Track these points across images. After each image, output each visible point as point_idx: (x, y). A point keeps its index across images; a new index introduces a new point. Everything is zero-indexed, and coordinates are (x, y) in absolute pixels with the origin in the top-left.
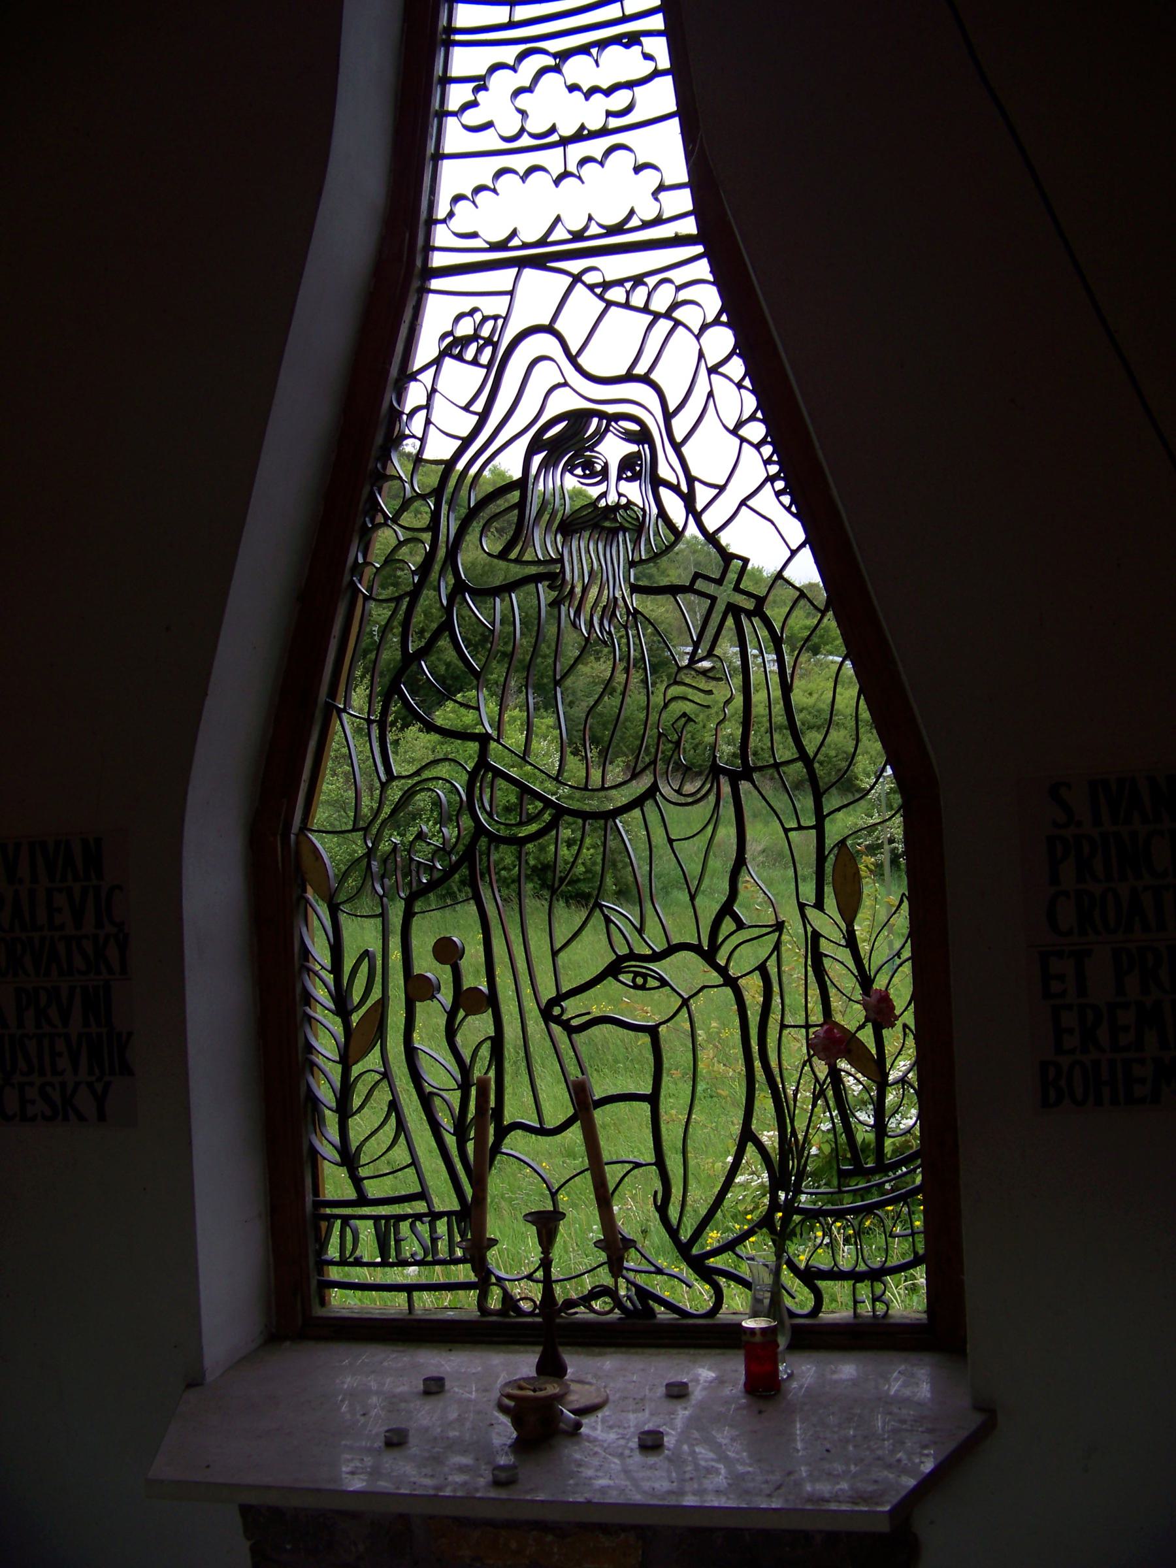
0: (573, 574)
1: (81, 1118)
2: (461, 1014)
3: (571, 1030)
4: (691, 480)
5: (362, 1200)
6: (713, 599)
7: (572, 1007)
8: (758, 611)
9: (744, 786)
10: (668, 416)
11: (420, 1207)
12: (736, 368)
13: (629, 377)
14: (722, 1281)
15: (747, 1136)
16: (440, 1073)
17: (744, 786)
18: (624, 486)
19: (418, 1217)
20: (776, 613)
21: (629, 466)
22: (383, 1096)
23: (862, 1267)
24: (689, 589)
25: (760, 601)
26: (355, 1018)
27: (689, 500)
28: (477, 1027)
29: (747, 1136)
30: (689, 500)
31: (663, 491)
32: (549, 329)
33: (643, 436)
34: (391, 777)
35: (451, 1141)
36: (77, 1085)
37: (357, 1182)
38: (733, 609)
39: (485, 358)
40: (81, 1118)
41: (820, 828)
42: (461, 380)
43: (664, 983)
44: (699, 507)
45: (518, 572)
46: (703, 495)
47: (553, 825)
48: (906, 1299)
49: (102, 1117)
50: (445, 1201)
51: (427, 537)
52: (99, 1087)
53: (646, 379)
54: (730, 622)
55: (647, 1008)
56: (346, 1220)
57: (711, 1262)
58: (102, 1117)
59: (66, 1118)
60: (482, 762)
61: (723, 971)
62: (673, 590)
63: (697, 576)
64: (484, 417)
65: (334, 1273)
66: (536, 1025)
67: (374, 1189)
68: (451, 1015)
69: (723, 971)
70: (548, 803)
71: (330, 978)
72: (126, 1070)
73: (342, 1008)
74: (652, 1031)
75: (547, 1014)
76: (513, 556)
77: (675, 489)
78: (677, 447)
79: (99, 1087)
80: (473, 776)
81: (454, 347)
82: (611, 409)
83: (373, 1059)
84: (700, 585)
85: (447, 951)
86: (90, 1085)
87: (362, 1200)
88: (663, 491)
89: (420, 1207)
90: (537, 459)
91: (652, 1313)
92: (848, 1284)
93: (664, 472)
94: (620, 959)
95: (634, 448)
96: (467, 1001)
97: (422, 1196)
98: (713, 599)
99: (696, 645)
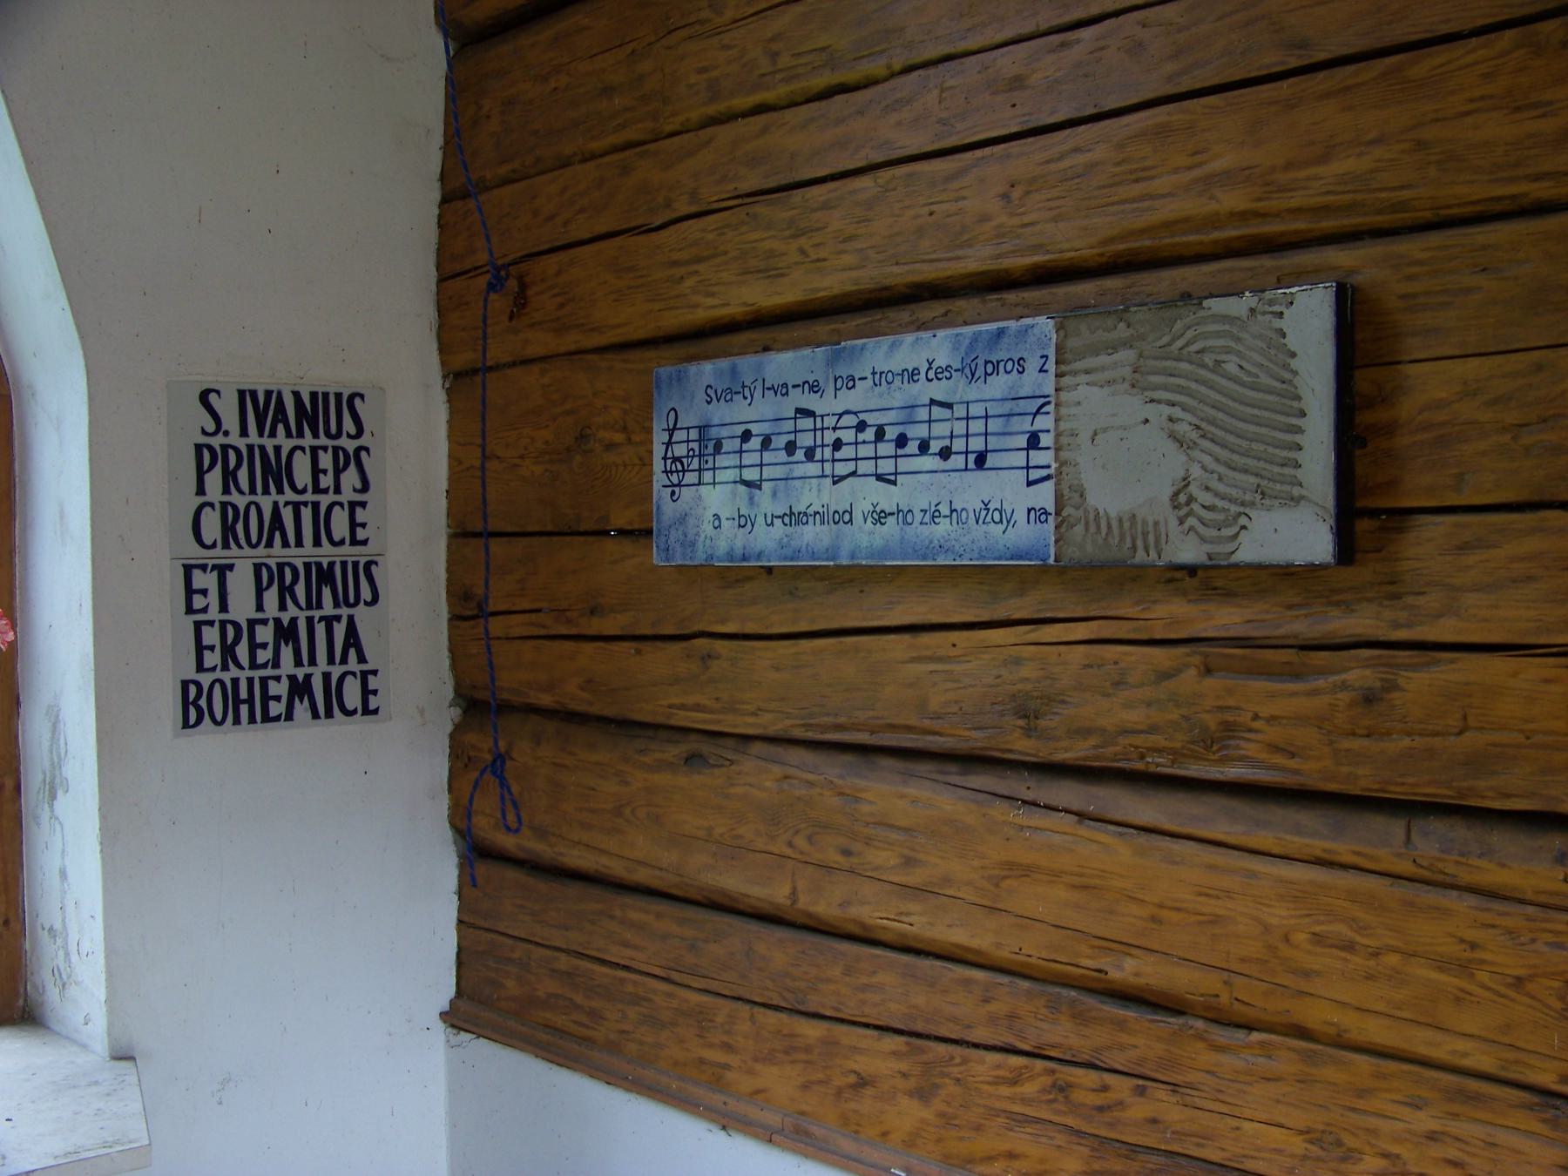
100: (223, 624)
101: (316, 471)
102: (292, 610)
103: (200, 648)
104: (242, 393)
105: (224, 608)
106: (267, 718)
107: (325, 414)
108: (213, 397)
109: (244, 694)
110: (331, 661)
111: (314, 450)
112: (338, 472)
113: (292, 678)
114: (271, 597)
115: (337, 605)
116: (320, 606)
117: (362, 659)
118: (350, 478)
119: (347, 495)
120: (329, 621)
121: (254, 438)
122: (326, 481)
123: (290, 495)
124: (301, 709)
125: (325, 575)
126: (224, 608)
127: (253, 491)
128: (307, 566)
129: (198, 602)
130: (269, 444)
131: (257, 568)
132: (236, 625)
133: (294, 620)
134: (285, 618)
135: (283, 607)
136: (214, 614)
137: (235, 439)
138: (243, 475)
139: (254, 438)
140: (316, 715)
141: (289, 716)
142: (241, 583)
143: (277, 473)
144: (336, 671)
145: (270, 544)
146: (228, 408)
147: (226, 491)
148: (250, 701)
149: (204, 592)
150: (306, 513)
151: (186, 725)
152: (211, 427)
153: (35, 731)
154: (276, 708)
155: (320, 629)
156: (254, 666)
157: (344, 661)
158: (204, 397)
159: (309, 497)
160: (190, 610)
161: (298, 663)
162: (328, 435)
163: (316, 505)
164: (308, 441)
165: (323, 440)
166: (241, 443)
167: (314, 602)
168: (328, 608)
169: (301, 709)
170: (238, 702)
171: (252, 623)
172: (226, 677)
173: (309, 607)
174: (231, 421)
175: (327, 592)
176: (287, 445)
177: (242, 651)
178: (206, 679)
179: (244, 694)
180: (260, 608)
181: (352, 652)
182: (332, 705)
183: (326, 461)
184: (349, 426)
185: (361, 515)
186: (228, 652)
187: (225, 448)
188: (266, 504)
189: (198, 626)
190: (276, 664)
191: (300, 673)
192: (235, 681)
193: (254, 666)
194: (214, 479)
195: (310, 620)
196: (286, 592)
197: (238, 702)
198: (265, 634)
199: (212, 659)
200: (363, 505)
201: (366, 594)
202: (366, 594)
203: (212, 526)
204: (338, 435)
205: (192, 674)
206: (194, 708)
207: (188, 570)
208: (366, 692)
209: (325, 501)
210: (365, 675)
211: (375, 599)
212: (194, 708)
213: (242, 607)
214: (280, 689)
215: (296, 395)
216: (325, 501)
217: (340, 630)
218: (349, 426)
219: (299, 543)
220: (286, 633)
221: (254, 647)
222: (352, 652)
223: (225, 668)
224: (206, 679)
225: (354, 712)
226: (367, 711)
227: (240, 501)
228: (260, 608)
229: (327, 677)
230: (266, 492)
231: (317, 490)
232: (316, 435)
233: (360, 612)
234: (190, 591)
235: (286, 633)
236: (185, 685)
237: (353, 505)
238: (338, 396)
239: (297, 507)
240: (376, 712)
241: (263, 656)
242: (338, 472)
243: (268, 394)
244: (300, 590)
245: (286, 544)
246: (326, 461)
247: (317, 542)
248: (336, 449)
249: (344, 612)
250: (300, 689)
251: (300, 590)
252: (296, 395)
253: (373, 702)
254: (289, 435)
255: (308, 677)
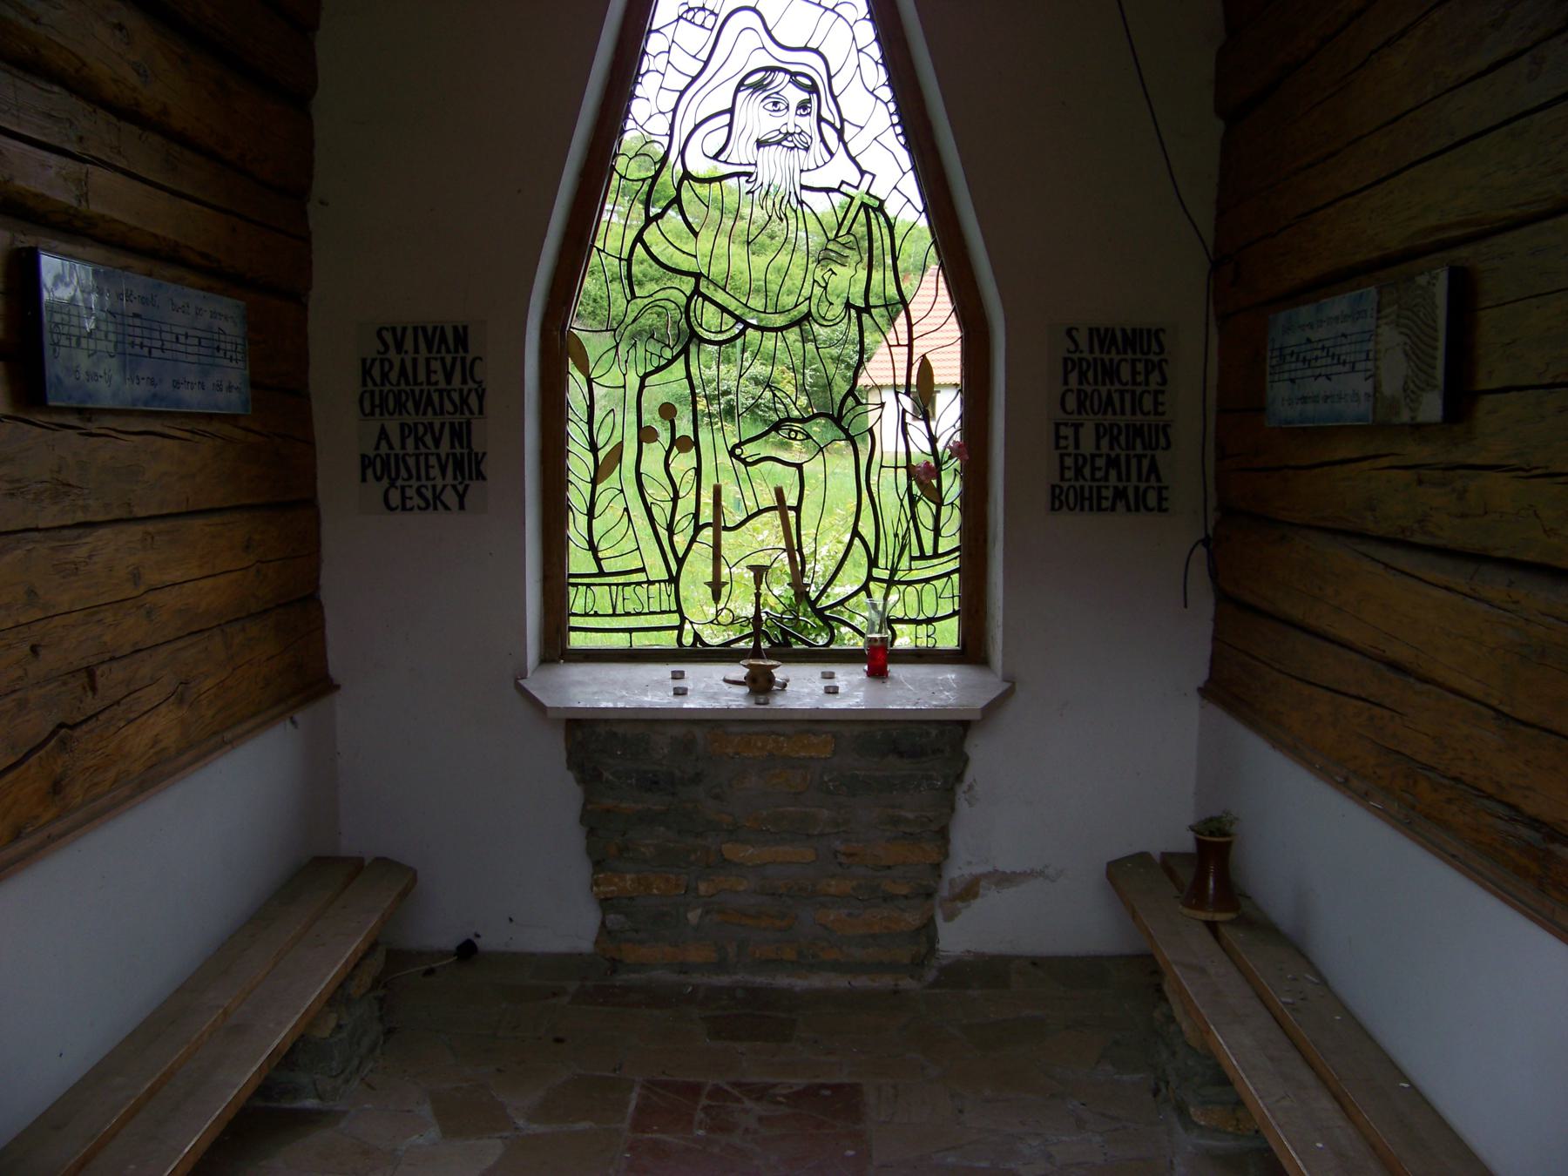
0: (764, 176)
1: (446, 508)
2: (675, 450)
3: (747, 464)
4: (842, 120)
5: (602, 573)
6: (852, 198)
7: (749, 451)
8: (880, 209)
9: (865, 317)
10: (830, 77)
11: (641, 577)
12: (875, 51)
13: (805, 49)
14: (835, 624)
15: (856, 533)
16: (658, 493)
17: (865, 317)
18: (799, 120)
19: (639, 584)
20: (891, 210)
21: (803, 106)
22: (619, 506)
23: (922, 617)
24: (838, 190)
25: (882, 202)
26: (602, 455)
27: (840, 133)
28: (683, 463)
29: (856, 533)
30: (840, 133)
31: (823, 125)
32: (754, 10)
33: (813, 89)
34: (634, 296)
35: (664, 534)
36: (444, 487)
37: (598, 561)
38: (864, 205)
39: (709, 24)
40: (446, 508)
41: (910, 346)
42: (693, 38)
43: (808, 437)
44: (847, 138)
45: (725, 169)
46: (849, 132)
47: (742, 332)
48: (948, 635)
49: (462, 507)
50: (657, 571)
51: (665, 141)
52: (460, 488)
53: (816, 51)
54: (862, 214)
55: (796, 453)
56: (588, 585)
57: (827, 613)
58: (462, 507)
59: (435, 508)
60: (696, 291)
61: (845, 431)
62: (828, 190)
63: (843, 182)
64: (706, 63)
65: (574, 622)
66: (724, 458)
67: (608, 566)
68: (668, 453)
69: (845, 431)
70: (738, 319)
71: (585, 428)
72: (481, 476)
73: (594, 448)
74: (799, 467)
75: (732, 453)
76: (722, 158)
77: (832, 125)
78: (834, 98)
79: (460, 488)
80: (689, 299)
81: (687, 15)
82: (793, 68)
83: (613, 480)
84: (844, 188)
85: (667, 411)
86: (454, 487)
87: (602, 573)
88: (823, 125)
89: (641, 577)
90: (741, 96)
91: (790, 645)
92: (912, 627)
93: (825, 114)
94: (782, 421)
95: (805, 96)
96: (680, 444)
97: (643, 570)
98: (852, 198)
99: (840, 226)
100: (1076, 456)
101: (1134, 373)
102: (1117, 450)
103: (1063, 468)
104: (1091, 330)
105: (1077, 446)
106: (1100, 509)
107: (1142, 343)
108: (1074, 333)
109: (1087, 494)
110: (1139, 479)
111: (1134, 362)
112: (1147, 374)
113: (1116, 488)
114: (1105, 442)
115: (1145, 448)
116: (1134, 448)
117: (1159, 479)
118: (1155, 377)
119: (1153, 387)
120: (1139, 458)
121: (1097, 354)
122: (1140, 378)
123: (1117, 386)
124: (1120, 505)
125: (1138, 431)
126: (1077, 446)
127: (1096, 382)
128: (1127, 426)
129: (1063, 443)
130: (1106, 358)
131: (1097, 426)
132: (1084, 457)
133: (1118, 456)
134: (1113, 454)
135: (1112, 448)
136: (1071, 449)
137: (1086, 355)
138: (1090, 375)
139: (1097, 354)
140: (1129, 509)
141: (1113, 508)
142: (1087, 434)
143: (1110, 373)
144: (1143, 486)
145: (1105, 413)
146: (1082, 338)
147: (1081, 383)
148: (1090, 499)
149: (1066, 438)
150: (1128, 397)
151: (1053, 509)
152: (1072, 348)
153: (1006, 457)
154: (1105, 504)
155: (1134, 462)
156: (1093, 479)
157: (1148, 480)
158: (1069, 332)
159: (1129, 387)
160: (1057, 447)
161: (1120, 479)
162: (1143, 352)
163: (1133, 393)
164: (1130, 355)
165: (1139, 356)
166: (1090, 357)
167: (1130, 446)
168: (1139, 450)
169: (1120, 505)
170: (1083, 498)
171: (1093, 456)
172: (1077, 485)
173: (1128, 448)
174: (1084, 345)
175: (1138, 441)
176: (1117, 358)
177: (1087, 471)
178: (1065, 485)
179: (1087, 494)
180: (1098, 447)
181: (1153, 477)
182: (1140, 504)
183: (1140, 367)
184: (1155, 347)
185: (1161, 398)
186: (1079, 472)
187: (1081, 360)
188: (1104, 390)
189: (1062, 456)
190: (1106, 478)
191: (1121, 485)
192: (1082, 488)
193: (1093, 479)
194: (1073, 377)
195: (1128, 456)
196: (1114, 440)
197: (1083, 498)
198: (1101, 462)
199: (1069, 474)
200: (1163, 392)
201: (1162, 442)
202: (1162, 442)
203: (1071, 402)
204: (1149, 352)
205: (1057, 481)
206: (1058, 500)
207: (1057, 425)
208: (1161, 499)
209: (1139, 390)
210: (1160, 490)
211: (1168, 446)
212: (1058, 500)
213: (1088, 447)
214: (1108, 493)
215: (1123, 331)
216: (1139, 390)
217: (1146, 463)
218: (1155, 347)
219: (1123, 413)
220: (1113, 462)
221: (1094, 469)
222: (1153, 477)
223: (1077, 479)
224: (1065, 485)
225: (1152, 510)
226: (1162, 510)
227: (1089, 389)
228: (1098, 447)
229: (1137, 489)
230: (1104, 384)
231: (1134, 383)
232: (1134, 352)
233: (1159, 454)
234: (1058, 437)
235: (1113, 462)
236: (1053, 487)
237: (1157, 393)
238: (1149, 331)
239: (1122, 393)
240: (1166, 510)
241: (1099, 474)
242: (1147, 374)
243: (1107, 330)
244: (1122, 439)
245: (1114, 413)
246: (1140, 367)
247: (1133, 413)
248: (1147, 361)
249: (1149, 452)
250: (1120, 494)
251: (1122, 439)
252: (1123, 331)
253: (1165, 505)
254: (1118, 352)
255: (1125, 488)
